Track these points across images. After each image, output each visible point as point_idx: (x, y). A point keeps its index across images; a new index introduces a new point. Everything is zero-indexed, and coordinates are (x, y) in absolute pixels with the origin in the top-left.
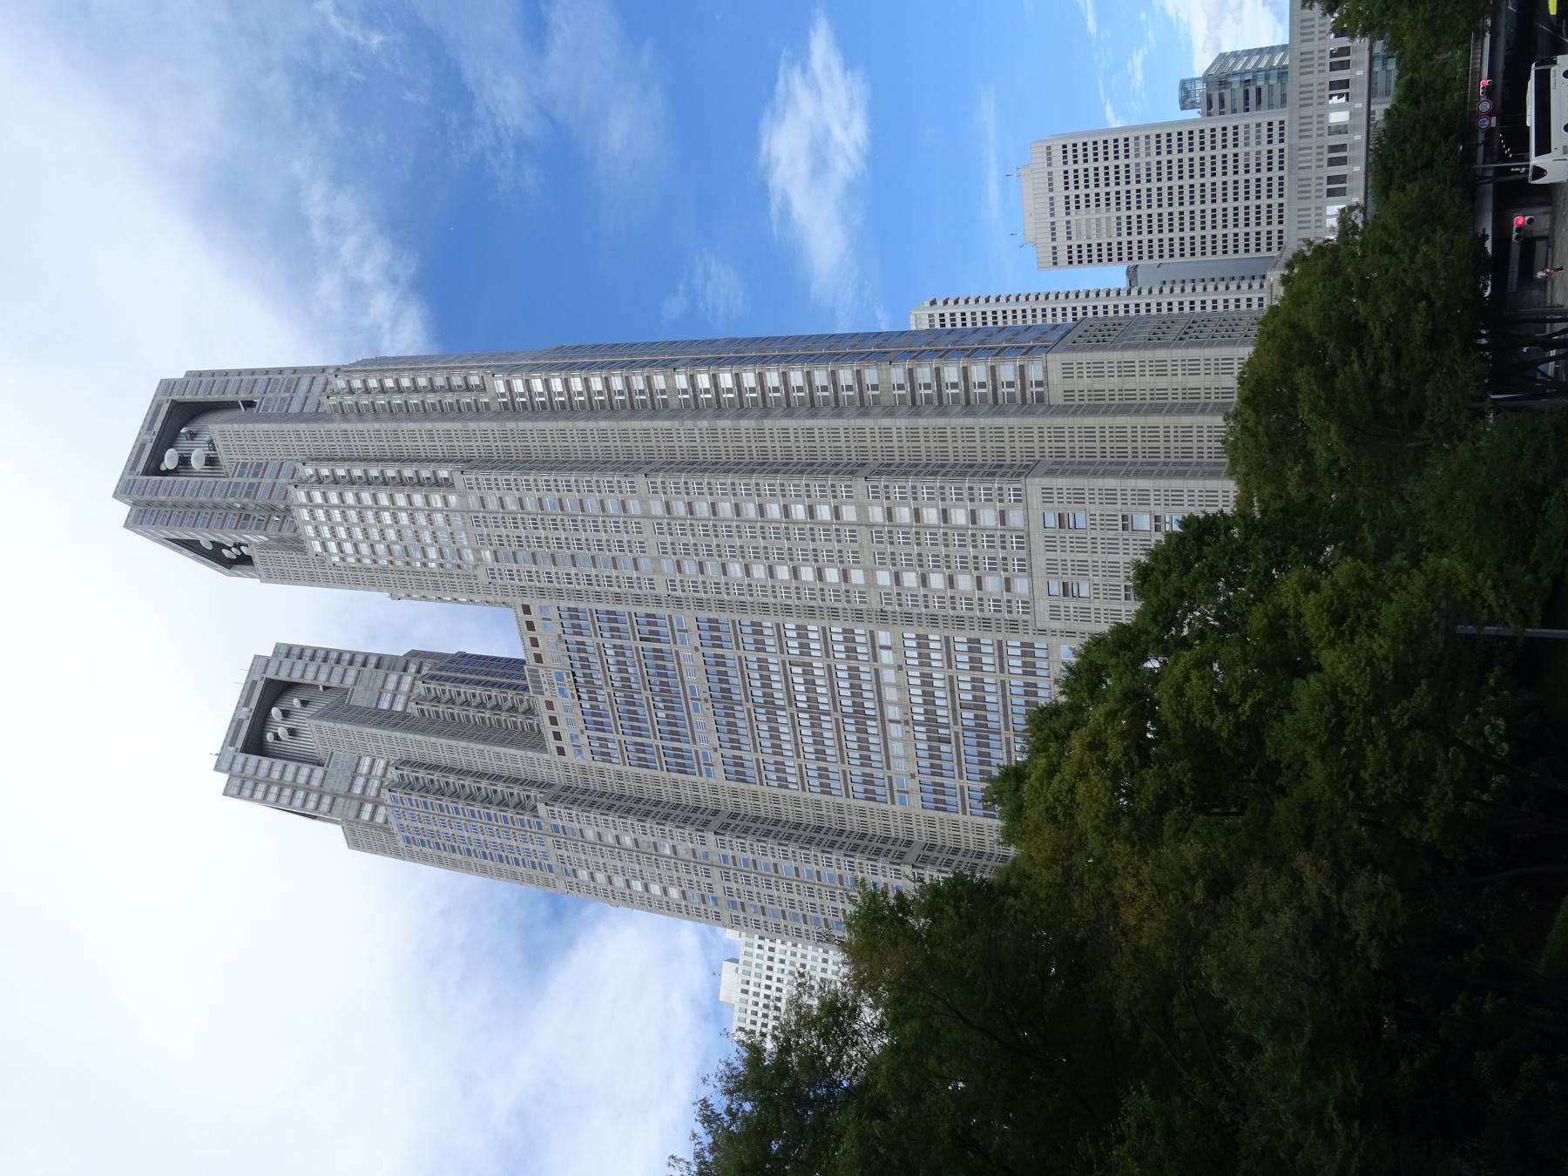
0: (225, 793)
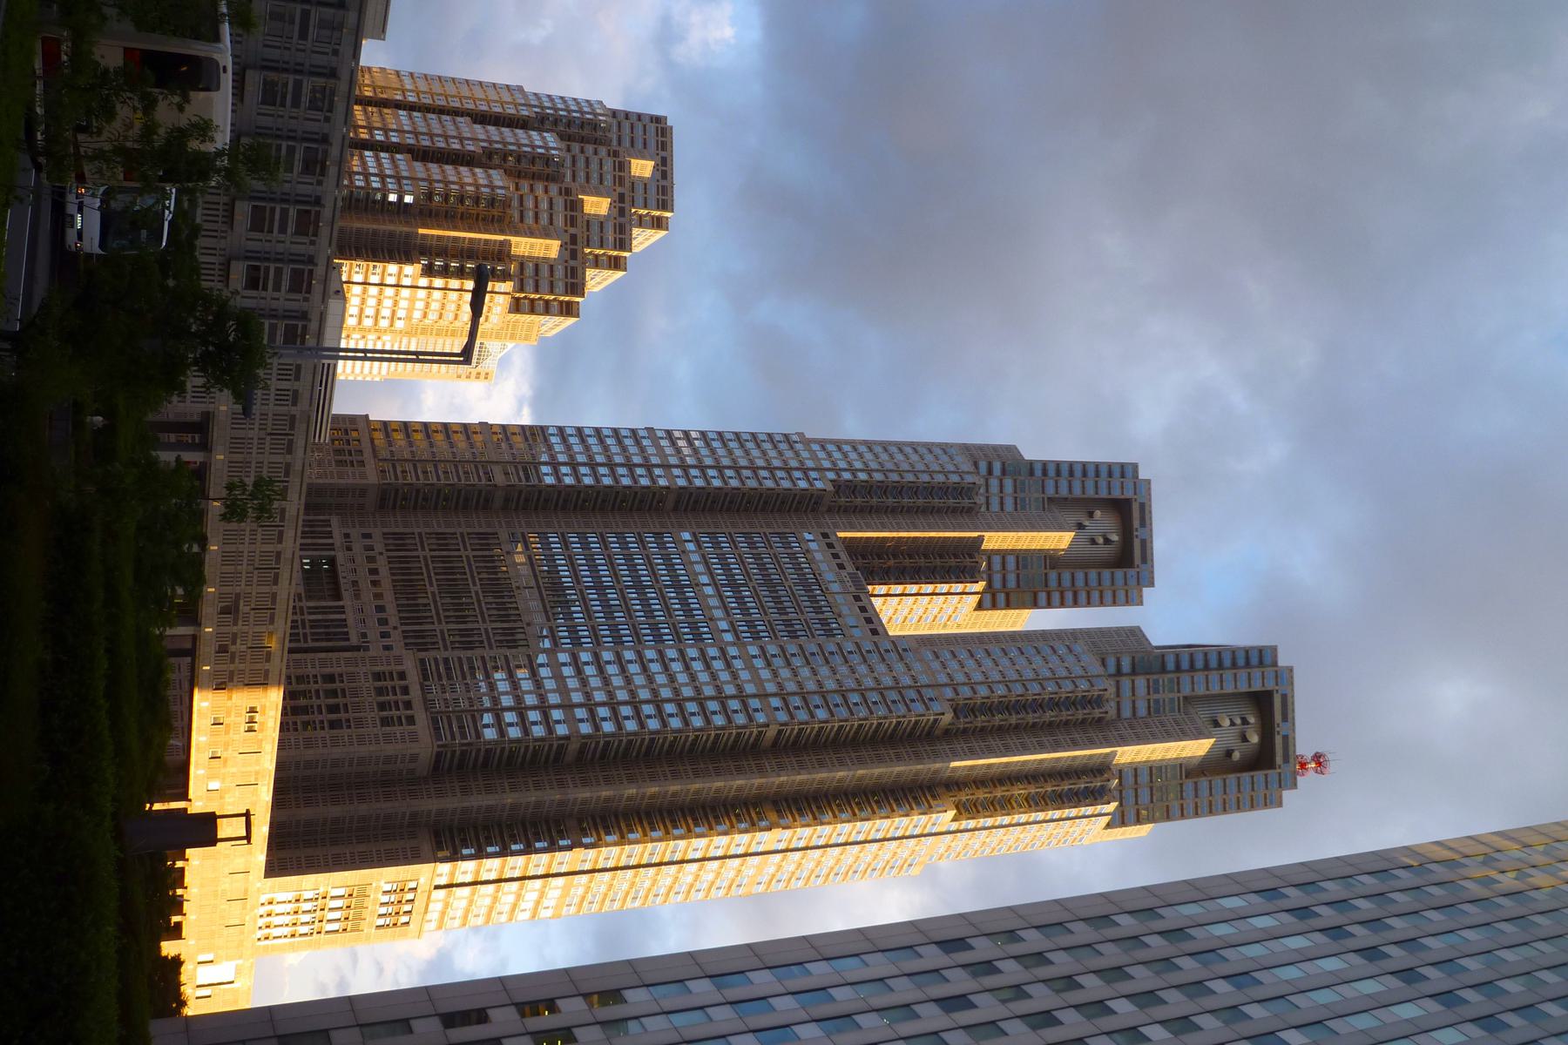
0: (1135, 467)
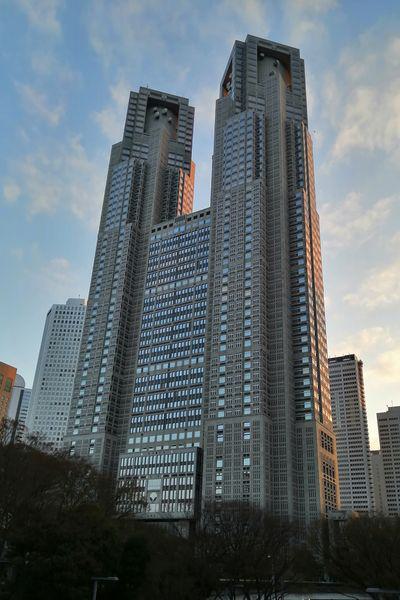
0: (131, 92)
